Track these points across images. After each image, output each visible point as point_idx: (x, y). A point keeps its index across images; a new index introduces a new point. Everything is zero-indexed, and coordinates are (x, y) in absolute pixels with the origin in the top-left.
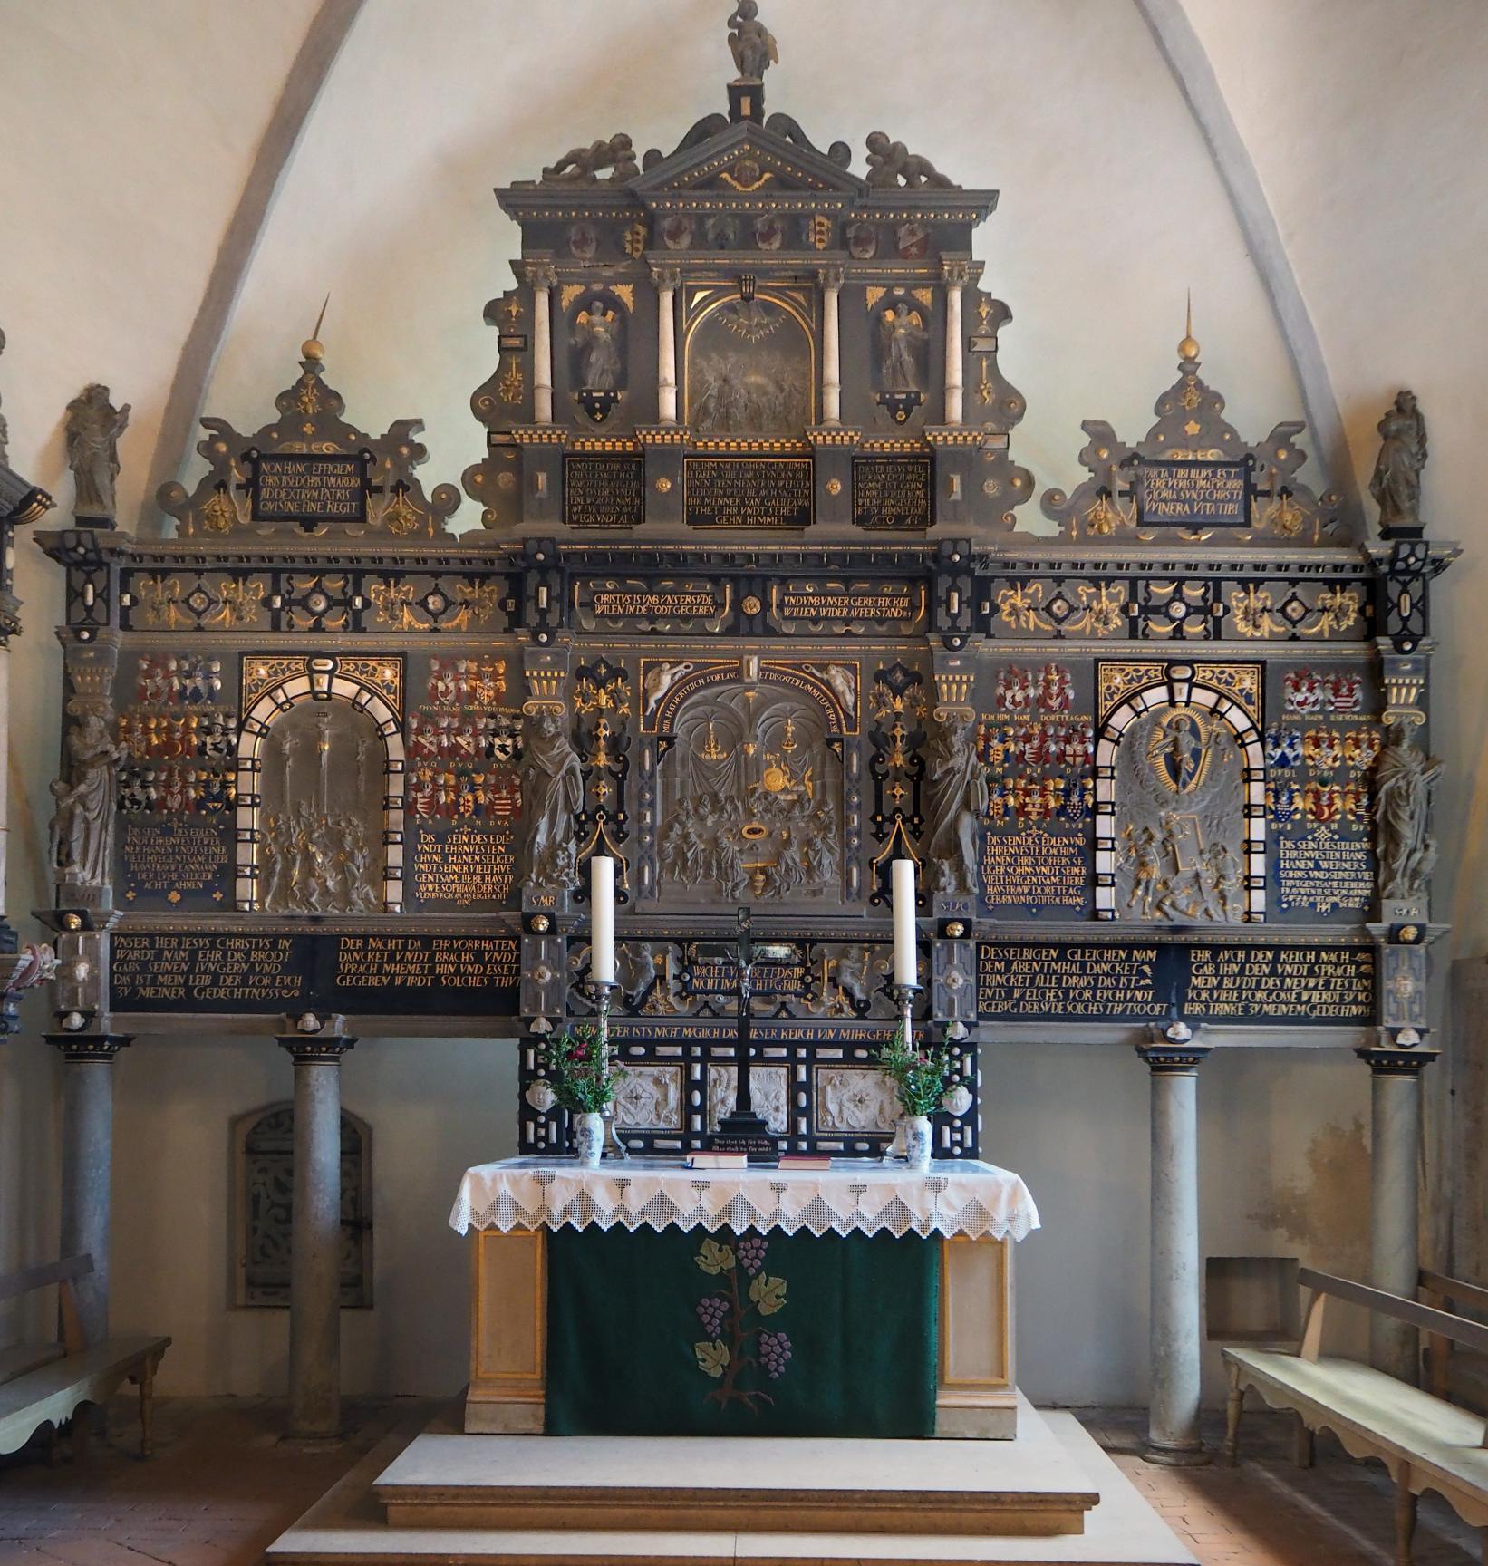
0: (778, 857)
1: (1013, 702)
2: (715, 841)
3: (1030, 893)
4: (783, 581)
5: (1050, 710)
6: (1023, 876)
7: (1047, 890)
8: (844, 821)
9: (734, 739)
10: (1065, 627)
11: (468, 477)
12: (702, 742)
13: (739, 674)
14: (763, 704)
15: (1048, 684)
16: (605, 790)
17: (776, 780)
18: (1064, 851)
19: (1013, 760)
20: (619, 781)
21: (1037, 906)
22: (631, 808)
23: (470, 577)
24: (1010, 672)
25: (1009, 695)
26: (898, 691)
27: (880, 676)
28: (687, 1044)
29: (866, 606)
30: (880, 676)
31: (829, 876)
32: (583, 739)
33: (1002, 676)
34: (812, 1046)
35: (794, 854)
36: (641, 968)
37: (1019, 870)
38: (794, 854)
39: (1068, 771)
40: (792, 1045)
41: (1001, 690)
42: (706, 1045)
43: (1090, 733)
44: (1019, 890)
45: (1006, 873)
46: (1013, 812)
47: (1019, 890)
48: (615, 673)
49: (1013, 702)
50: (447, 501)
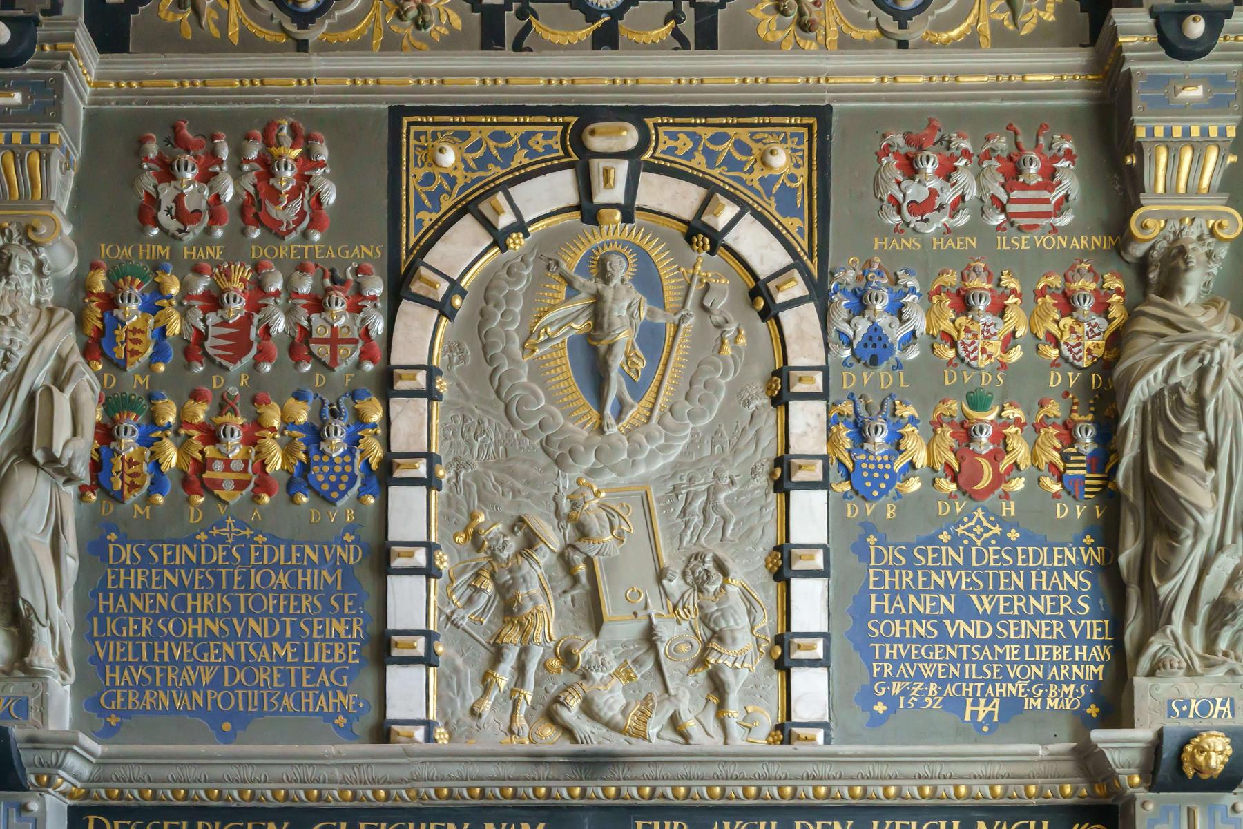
1: (180, 213)
3: (216, 683)
5: (275, 231)
6: (201, 643)
7: (261, 676)
10: (314, 34)
15: (268, 167)
18: (306, 578)
19: (174, 354)
21: (233, 716)
24: (176, 140)
25: (167, 194)
33: (153, 149)
37: (188, 628)
39: (319, 379)
41: (148, 181)
43: (377, 288)
44: (190, 675)
45: (157, 635)
46: (171, 484)
47: (190, 675)
49: (180, 213)
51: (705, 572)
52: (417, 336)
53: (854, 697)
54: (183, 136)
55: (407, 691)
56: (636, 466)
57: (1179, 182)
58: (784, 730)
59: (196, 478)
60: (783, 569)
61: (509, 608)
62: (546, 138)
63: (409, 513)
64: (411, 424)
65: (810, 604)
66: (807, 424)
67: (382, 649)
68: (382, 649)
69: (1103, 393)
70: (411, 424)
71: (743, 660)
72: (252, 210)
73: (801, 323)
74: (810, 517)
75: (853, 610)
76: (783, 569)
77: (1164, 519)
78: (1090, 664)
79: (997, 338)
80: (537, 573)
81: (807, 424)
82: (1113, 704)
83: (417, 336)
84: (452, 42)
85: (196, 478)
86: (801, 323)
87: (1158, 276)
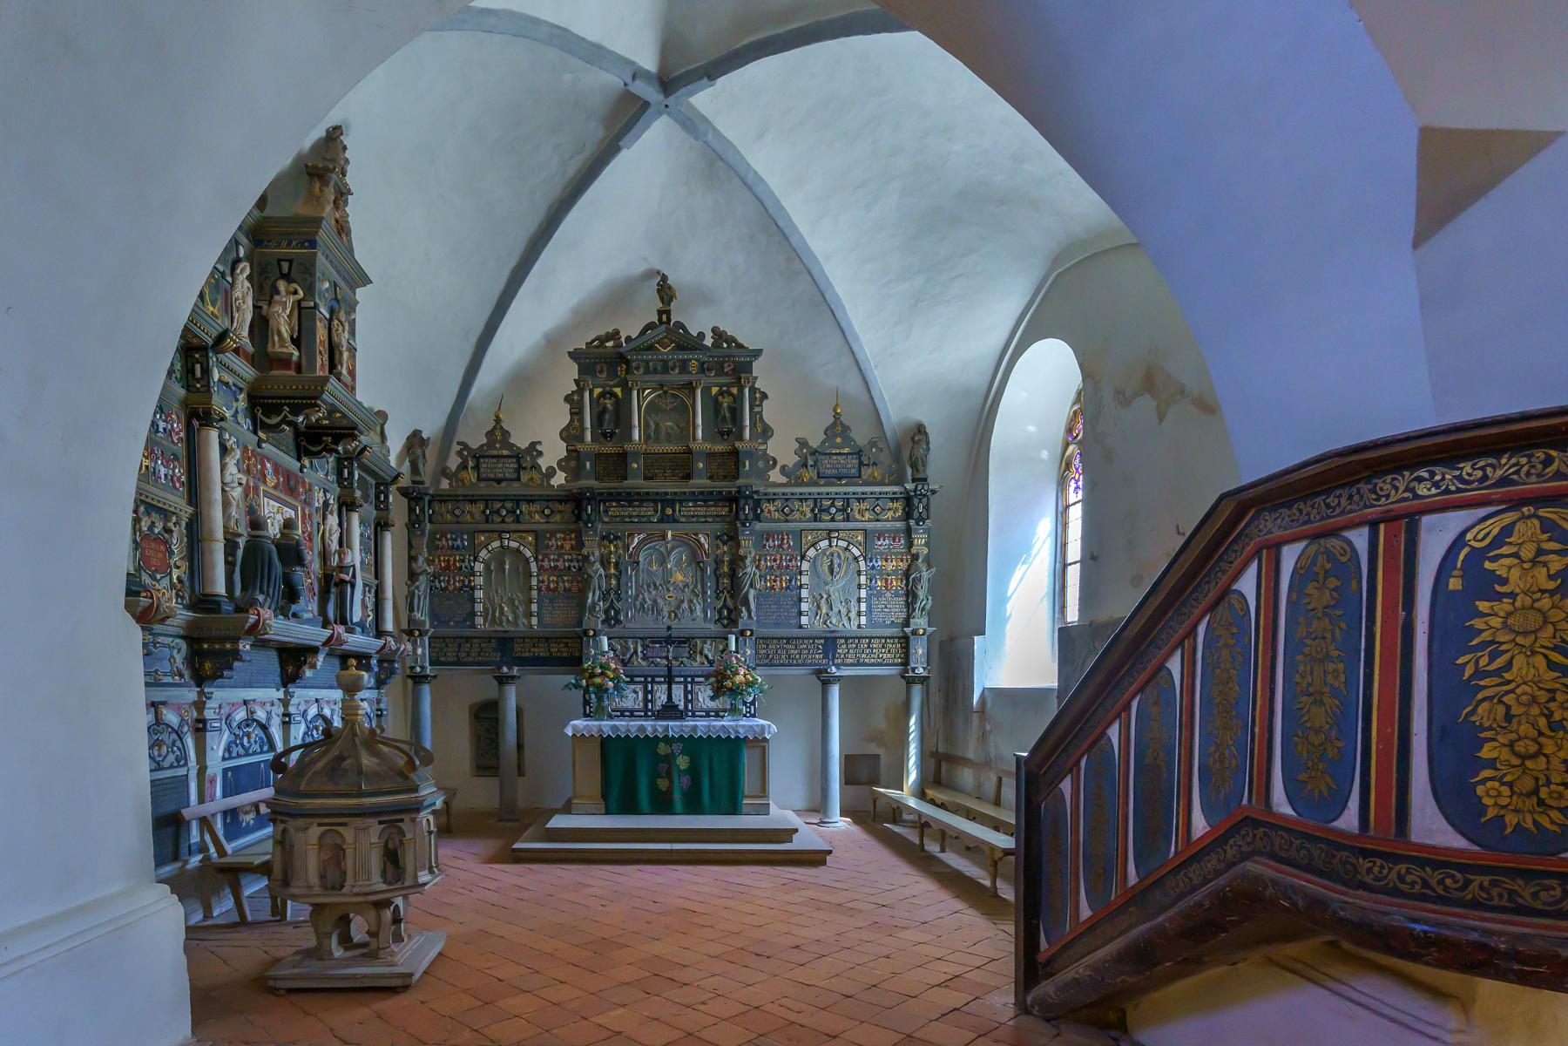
0: (679, 607)
2: (655, 601)
4: (681, 502)
8: (704, 593)
9: (663, 561)
11: (559, 463)
12: (650, 563)
13: (664, 537)
14: (673, 549)
16: (614, 582)
17: (679, 577)
20: (619, 580)
22: (623, 588)
23: (560, 502)
26: (725, 543)
27: (718, 538)
28: (646, 677)
29: (712, 511)
30: (718, 538)
31: (699, 613)
32: (605, 563)
34: (693, 677)
35: (685, 605)
36: (628, 649)
38: (685, 605)
40: (685, 677)
42: (653, 677)
48: (617, 538)
50: (551, 472)
51: (847, 602)
52: (805, 566)
53: (869, 620)
54: (769, 535)
55: (804, 620)
56: (835, 589)
57: (920, 541)
58: (859, 626)
59: (772, 588)
60: (859, 601)
61: (819, 607)
62: (824, 534)
63: (804, 593)
64: (805, 579)
65: (863, 607)
66: (863, 579)
67: (800, 613)
68: (800, 613)
69: (907, 574)
70: (805, 579)
71: (853, 615)
72: (780, 546)
73: (862, 564)
74: (863, 593)
75: (869, 607)
76: (859, 601)
77: (915, 596)
78: (904, 616)
79: (890, 566)
80: (823, 602)
81: (863, 579)
82: (907, 623)
83: (805, 566)
84: (809, 521)
85: (772, 588)
86: (862, 564)
87: (915, 557)
